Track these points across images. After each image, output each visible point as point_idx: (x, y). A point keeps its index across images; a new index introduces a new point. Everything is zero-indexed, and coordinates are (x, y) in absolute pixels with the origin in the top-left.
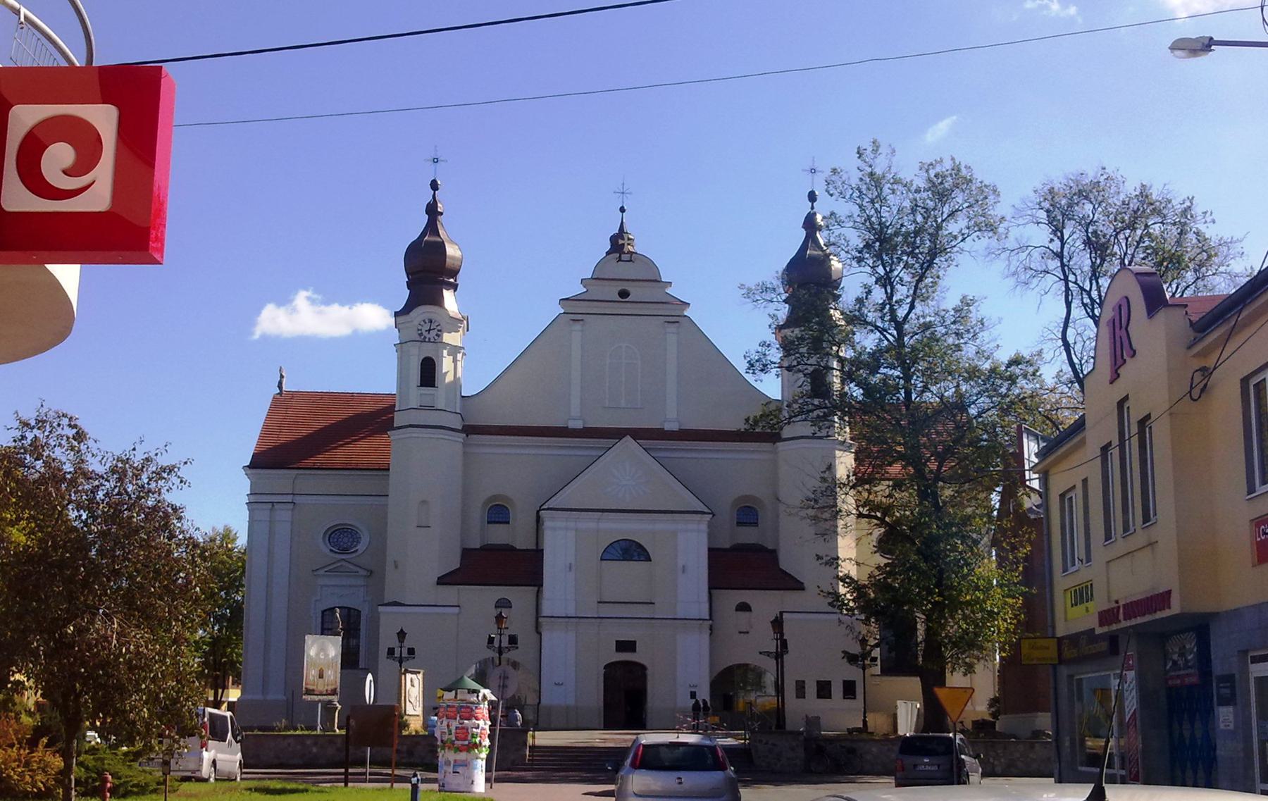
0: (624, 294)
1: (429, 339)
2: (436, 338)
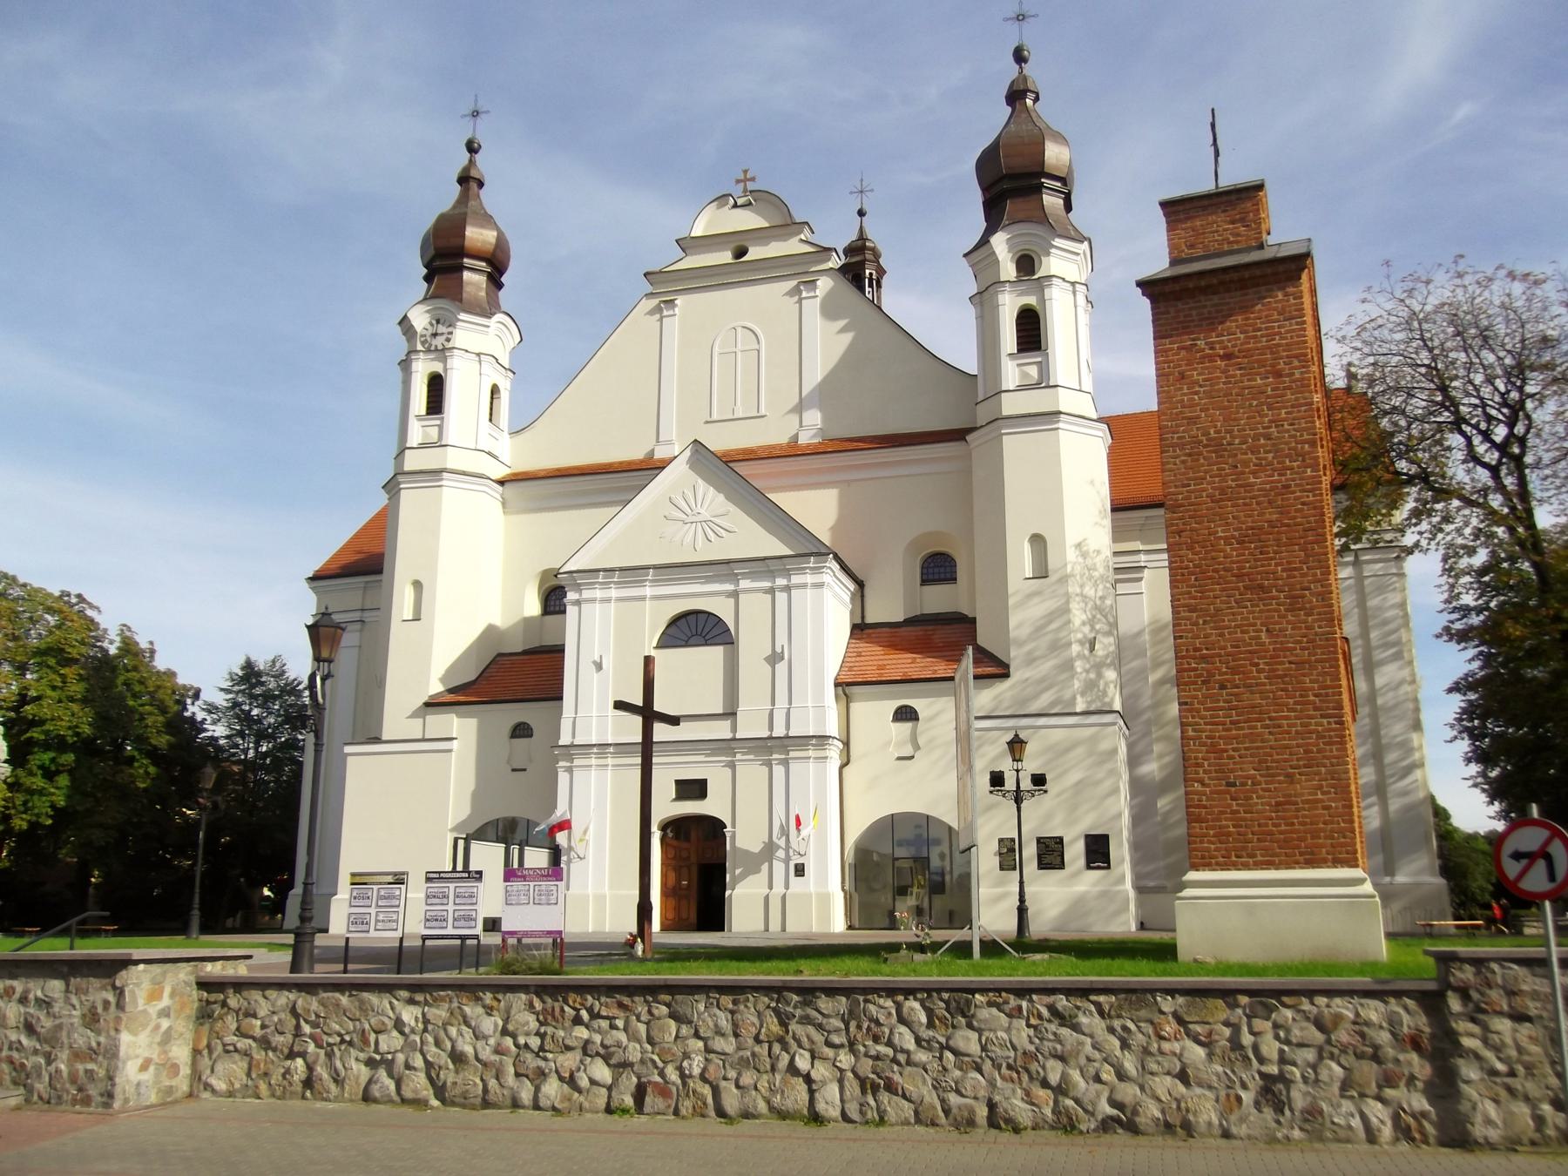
1: (436, 346)
2: (445, 343)
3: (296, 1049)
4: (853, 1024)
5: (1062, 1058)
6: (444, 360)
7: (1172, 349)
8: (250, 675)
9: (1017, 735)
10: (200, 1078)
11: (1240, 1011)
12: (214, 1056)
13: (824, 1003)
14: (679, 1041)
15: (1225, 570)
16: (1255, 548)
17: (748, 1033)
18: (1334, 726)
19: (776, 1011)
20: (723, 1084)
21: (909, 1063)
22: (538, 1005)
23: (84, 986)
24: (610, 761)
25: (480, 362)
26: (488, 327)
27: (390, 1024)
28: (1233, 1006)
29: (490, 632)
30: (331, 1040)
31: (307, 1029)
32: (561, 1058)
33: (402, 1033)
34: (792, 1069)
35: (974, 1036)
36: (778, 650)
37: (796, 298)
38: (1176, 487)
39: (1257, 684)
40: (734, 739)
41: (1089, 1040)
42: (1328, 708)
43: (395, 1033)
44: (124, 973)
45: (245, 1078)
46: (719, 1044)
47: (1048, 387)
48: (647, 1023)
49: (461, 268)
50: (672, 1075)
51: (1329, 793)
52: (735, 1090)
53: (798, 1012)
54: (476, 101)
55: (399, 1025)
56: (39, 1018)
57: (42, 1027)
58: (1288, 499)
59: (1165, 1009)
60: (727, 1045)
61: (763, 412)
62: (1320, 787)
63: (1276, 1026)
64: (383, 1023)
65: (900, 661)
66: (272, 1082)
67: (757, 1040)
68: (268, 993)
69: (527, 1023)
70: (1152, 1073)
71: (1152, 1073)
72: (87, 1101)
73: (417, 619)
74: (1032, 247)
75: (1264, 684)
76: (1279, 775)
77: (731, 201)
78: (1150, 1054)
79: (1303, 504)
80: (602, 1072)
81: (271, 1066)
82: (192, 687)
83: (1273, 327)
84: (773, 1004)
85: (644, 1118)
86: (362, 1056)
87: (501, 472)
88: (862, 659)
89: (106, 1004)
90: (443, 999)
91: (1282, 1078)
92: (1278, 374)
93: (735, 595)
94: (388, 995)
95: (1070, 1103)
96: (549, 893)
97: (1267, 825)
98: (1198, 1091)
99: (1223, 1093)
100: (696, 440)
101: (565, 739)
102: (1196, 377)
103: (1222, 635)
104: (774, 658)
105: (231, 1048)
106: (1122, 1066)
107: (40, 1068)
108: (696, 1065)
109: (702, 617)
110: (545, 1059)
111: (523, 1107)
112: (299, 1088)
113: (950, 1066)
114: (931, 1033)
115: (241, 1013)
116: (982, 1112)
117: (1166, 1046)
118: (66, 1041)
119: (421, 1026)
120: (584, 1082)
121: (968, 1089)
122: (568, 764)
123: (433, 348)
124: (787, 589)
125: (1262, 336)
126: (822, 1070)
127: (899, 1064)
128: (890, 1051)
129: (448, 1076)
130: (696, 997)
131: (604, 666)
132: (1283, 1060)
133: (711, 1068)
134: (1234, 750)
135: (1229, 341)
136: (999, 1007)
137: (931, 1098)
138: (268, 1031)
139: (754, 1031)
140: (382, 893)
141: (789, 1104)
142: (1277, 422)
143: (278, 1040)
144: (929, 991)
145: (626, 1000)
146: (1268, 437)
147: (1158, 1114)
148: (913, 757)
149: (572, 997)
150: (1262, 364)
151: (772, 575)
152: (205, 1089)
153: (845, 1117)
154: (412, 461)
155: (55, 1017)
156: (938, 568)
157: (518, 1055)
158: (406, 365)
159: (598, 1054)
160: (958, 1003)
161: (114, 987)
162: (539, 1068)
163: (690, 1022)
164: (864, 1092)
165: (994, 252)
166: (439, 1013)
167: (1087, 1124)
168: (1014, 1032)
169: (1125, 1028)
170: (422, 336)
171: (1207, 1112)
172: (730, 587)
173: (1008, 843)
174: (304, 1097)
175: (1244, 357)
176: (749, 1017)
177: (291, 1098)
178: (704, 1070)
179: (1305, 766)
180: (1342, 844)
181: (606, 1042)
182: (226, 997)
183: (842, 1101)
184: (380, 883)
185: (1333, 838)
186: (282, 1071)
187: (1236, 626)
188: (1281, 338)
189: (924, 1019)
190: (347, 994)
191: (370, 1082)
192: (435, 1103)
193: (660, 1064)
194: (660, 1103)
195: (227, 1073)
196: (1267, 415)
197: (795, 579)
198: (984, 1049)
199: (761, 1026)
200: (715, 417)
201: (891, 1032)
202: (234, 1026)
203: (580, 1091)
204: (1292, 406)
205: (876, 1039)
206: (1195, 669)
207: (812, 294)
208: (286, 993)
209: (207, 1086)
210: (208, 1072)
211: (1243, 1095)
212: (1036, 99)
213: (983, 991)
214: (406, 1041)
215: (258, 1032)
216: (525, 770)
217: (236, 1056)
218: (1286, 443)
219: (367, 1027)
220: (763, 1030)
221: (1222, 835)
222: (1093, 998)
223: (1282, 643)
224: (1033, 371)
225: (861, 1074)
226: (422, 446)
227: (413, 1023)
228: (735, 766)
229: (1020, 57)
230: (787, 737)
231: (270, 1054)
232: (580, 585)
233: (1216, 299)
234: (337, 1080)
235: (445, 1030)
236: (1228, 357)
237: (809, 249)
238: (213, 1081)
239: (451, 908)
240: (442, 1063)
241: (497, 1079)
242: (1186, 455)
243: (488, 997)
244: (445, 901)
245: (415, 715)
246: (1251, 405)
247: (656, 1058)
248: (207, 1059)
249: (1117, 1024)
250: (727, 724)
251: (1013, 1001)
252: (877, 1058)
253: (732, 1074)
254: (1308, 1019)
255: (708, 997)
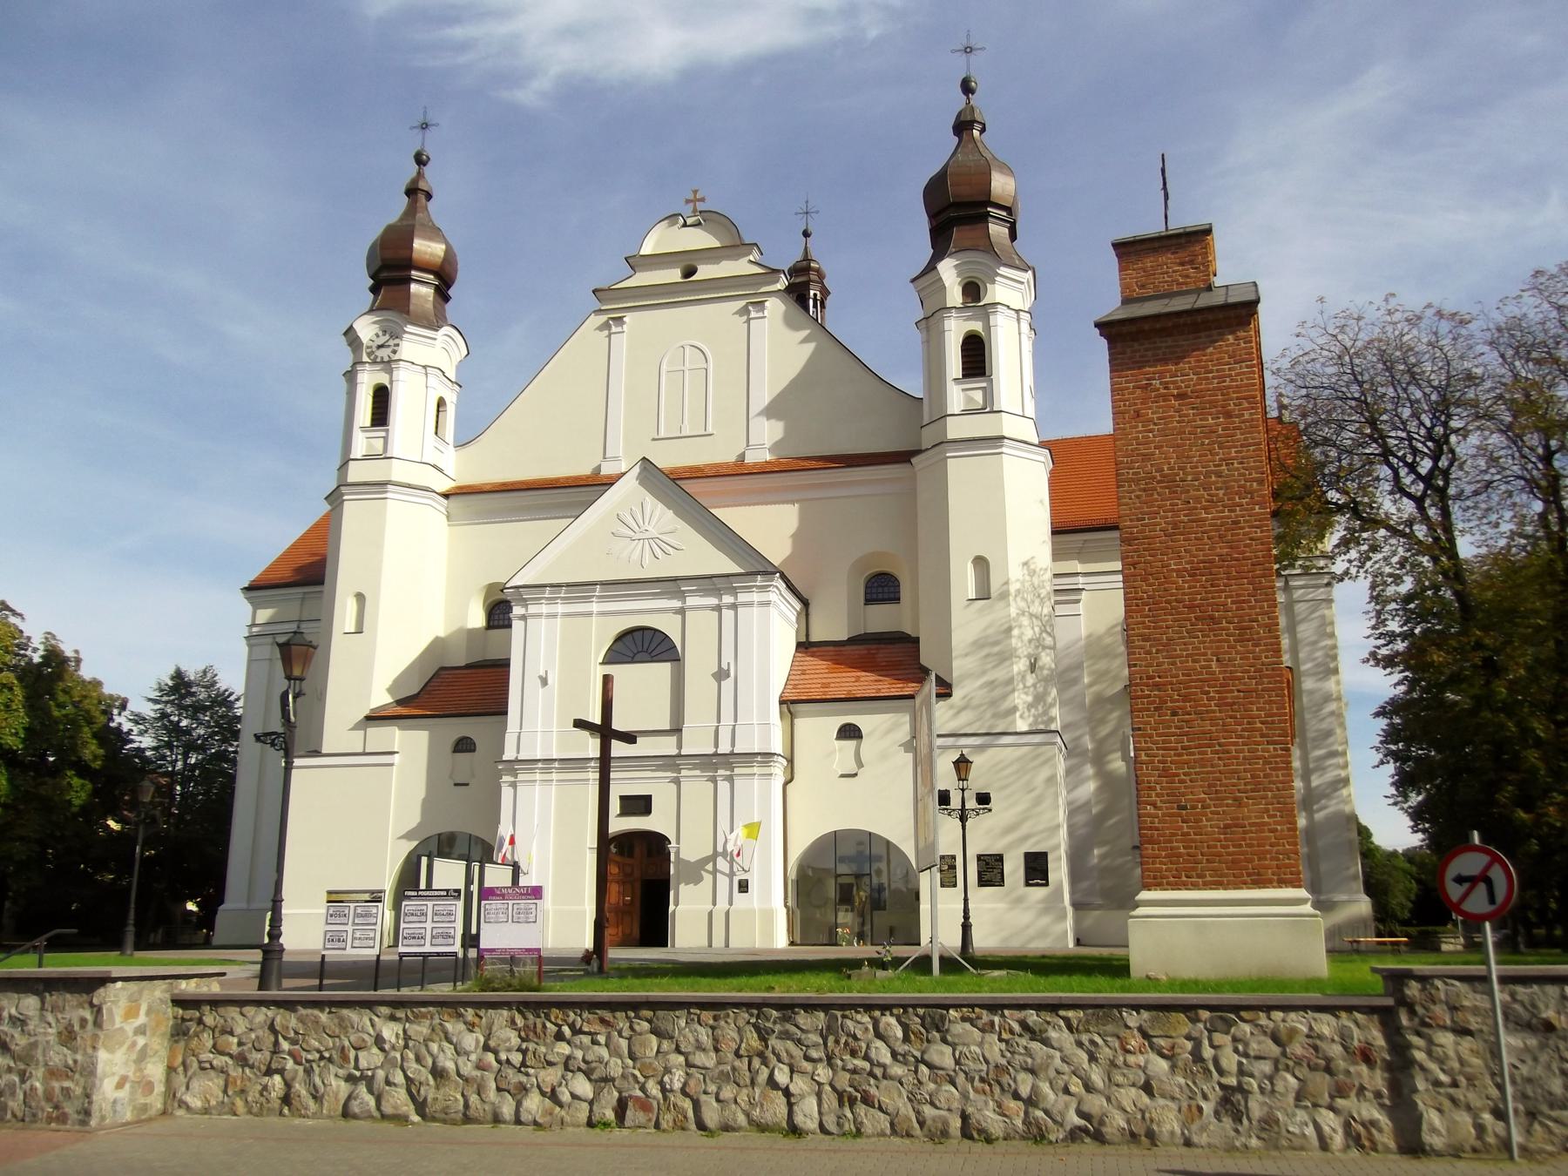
0: (689, 272)
1: (382, 358)
2: (392, 355)
3: (274, 1066)
4: (831, 1039)
5: (1032, 1071)
6: (390, 372)
7: (1128, 388)
8: (180, 686)
9: (962, 755)
10: (174, 1095)
11: (1201, 1026)
12: (189, 1073)
13: (802, 1018)
14: (660, 1055)
15: (1177, 601)
16: (1206, 581)
17: (728, 1049)
18: (1280, 752)
19: (756, 1027)
20: (703, 1098)
21: (885, 1076)
22: (520, 1021)
23: (60, 1003)
24: (554, 776)
25: (426, 374)
26: (435, 339)
27: (370, 1041)
28: (1195, 1020)
29: (437, 645)
30: (310, 1057)
31: (285, 1045)
32: (542, 1073)
33: (382, 1049)
34: (772, 1083)
35: (948, 1050)
36: (724, 666)
37: (745, 318)
38: (1131, 520)
39: (1207, 712)
40: (679, 756)
41: (1058, 1054)
42: (1274, 735)
43: (375, 1050)
44: (101, 991)
45: (221, 1095)
46: (700, 1059)
47: (992, 412)
48: (629, 1039)
49: (409, 280)
50: (654, 1089)
51: (1275, 816)
52: (715, 1104)
53: (777, 1028)
54: (425, 112)
55: (379, 1041)
56: (13, 1036)
57: (16, 1045)
58: (1238, 534)
59: (1131, 1024)
60: (707, 1060)
61: (710, 430)
62: (1267, 811)
63: (1235, 1040)
64: (363, 1040)
65: (844, 680)
66: (250, 1099)
67: (737, 1055)
68: (246, 1009)
69: (509, 1039)
70: (1118, 1085)
71: (1118, 1085)
72: (63, 1118)
73: (359, 631)
74: (976, 275)
75: (1214, 712)
76: (1228, 798)
77: (681, 221)
78: (1116, 1066)
79: (1251, 539)
80: (583, 1087)
81: (248, 1083)
82: (119, 698)
83: (1224, 370)
84: (753, 1020)
85: (625, 1132)
86: (341, 1072)
87: (445, 485)
88: (807, 677)
89: (83, 1022)
90: (424, 1016)
91: (1240, 1089)
92: (1228, 415)
93: (682, 612)
94: (368, 1011)
95: (1039, 1114)
96: (528, 912)
97: (1216, 847)
98: (1161, 1101)
99: (1185, 1105)
100: (644, 458)
101: (509, 754)
102: (1150, 415)
103: (1174, 664)
104: (721, 675)
105: (208, 1065)
106: (1089, 1078)
107: (14, 1085)
108: (676, 1080)
109: (648, 634)
110: (527, 1074)
111: (504, 1122)
112: (276, 1104)
113: (925, 1080)
114: (906, 1048)
115: (217, 1031)
116: (956, 1123)
117: (1131, 1059)
118: (41, 1058)
119: (401, 1042)
120: (565, 1097)
121: (942, 1100)
122: (513, 779)
123: (379, 360)
124: (734, 607)
125: (1213, 378)
126: (800, 1083)
127: (875, 1077)
128: (867, 1065)
129: (429, 1092)
130: (677, 1013)
131: (550, 682)
132: (1241, 1072)
133: (692, 1083)
134: (1185, 774)
135: (1182, 381)
136: (972, 1022)
137: (906, 1110)
138: (245, 1048)
139: (734, 1046)
140: (359, 910)
141: (768, 1117)
142: (1228, 461)
143: (255, 1057)
144: (905, 1007)
145: (607, 1015)
146: (1219, 474)
147: (1123, 1124)
148: (856, 775)
149: (555, 1011)
150: (1213, 404)
151: (718, 593)
152: (179, 1106)
153: (823, 1129)
154: (356, 473)
155: (30, 1035)
156: (882, 588)
157: (500, 1070)
158: (351, 376)
159: (579, 1069)
160: (933, 1018)
161: (92, 1005)
162: (520, 1083)
163: (671, 1038)
164: (841, 1104)
165: (941, 278)
166: (420, 1030)
167: (1056, 1134)
168: (986, 1046)
169: (1092, 1042)
170: (368, 347)
171: (1169, 1121)
172: (676, 604)
173: (949, 861)
174: (281, 1114)
175: (1197, 397)
176: (729, 1032)
177: (268, 1115)
178: (685, 1084)
179: (1253, 791)
180: (1287, 866)
181: (587, 1058)
182: (202, 1015)
183: (820, 1113)
184: (357, 901)
185: (1278, 859)
186: (259, 1088)
187: (1187, 656)
188: (1232, 380)
189: (900, 1034)
190: (327, 1010)
191: (350, 1098)
192: (416, 1118)
193: (641, 1079)
194: (641, 1117)
195: (203, 1090)
196: (1218, 454)
197: (742, 597)
198: (957, 1062)
199: (742, 1041)
200: (662, 435)
201: (868, 1047)
202: (210, 1044)
203: (561, 1105)
204: (1242, 446)
205: (853, 1053)
206: (1149, 696)
207: (760, 314)
208: (264, 1009)
209: (183, 1104)
210: (183, 1089)
211: (1204, 1104)
212: (983, 131)
213: (957, 1007)
214: (386, 1057)
215: (235, 1049)
216: (467, 785)
217: (212, 1073)
218: (1235, 481)
219: (347, 1043)
220: (743, 1045)
221: (1173, 856)
222: (1062, 1013)
223: (1231, 672)
224: (978, 396)
225: (839, 1087)
226: (367, 458)
227: (393, 1040)
228: (680, 782)
229: (967, 88)
230: (732, 754)
231: (247, 1070)
232: (526, 600)
233: (1170, 341)
234: (317, 1097)
235: (427, 1046)
236: (1181, 396)
237: (760, 270)
238: (188, 1098)
239: (429, 925)
240: (423, 1079)
241: (479, 1094)
242: (1140, 490)
243: (469, 1013)
244: (423, 918)
245: (357, 727)
246: (1203, 444)
247: (637, 1073)
248: (182, 1077)
249: (1085, 1038)
250: (673, 739)
251: (986, 1016)
252: (854, 1071)
253: (712, 1088)
254: (1265, 1033)
255: (689, 1013)
